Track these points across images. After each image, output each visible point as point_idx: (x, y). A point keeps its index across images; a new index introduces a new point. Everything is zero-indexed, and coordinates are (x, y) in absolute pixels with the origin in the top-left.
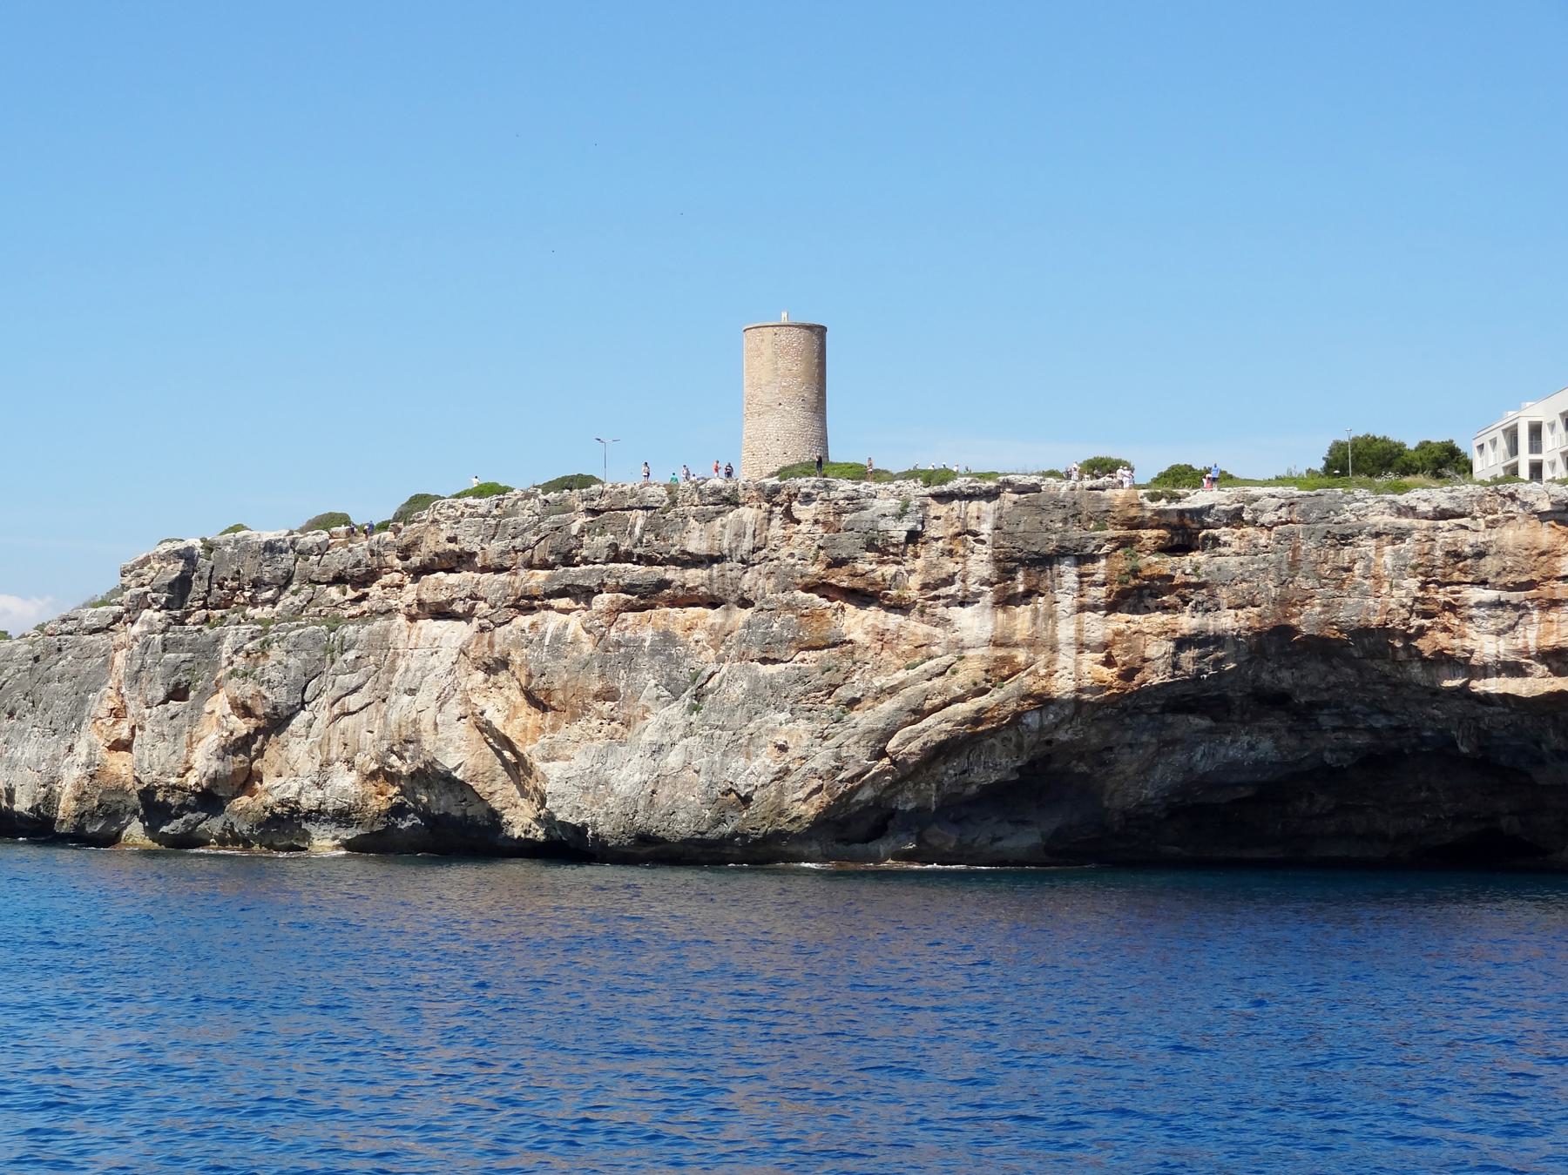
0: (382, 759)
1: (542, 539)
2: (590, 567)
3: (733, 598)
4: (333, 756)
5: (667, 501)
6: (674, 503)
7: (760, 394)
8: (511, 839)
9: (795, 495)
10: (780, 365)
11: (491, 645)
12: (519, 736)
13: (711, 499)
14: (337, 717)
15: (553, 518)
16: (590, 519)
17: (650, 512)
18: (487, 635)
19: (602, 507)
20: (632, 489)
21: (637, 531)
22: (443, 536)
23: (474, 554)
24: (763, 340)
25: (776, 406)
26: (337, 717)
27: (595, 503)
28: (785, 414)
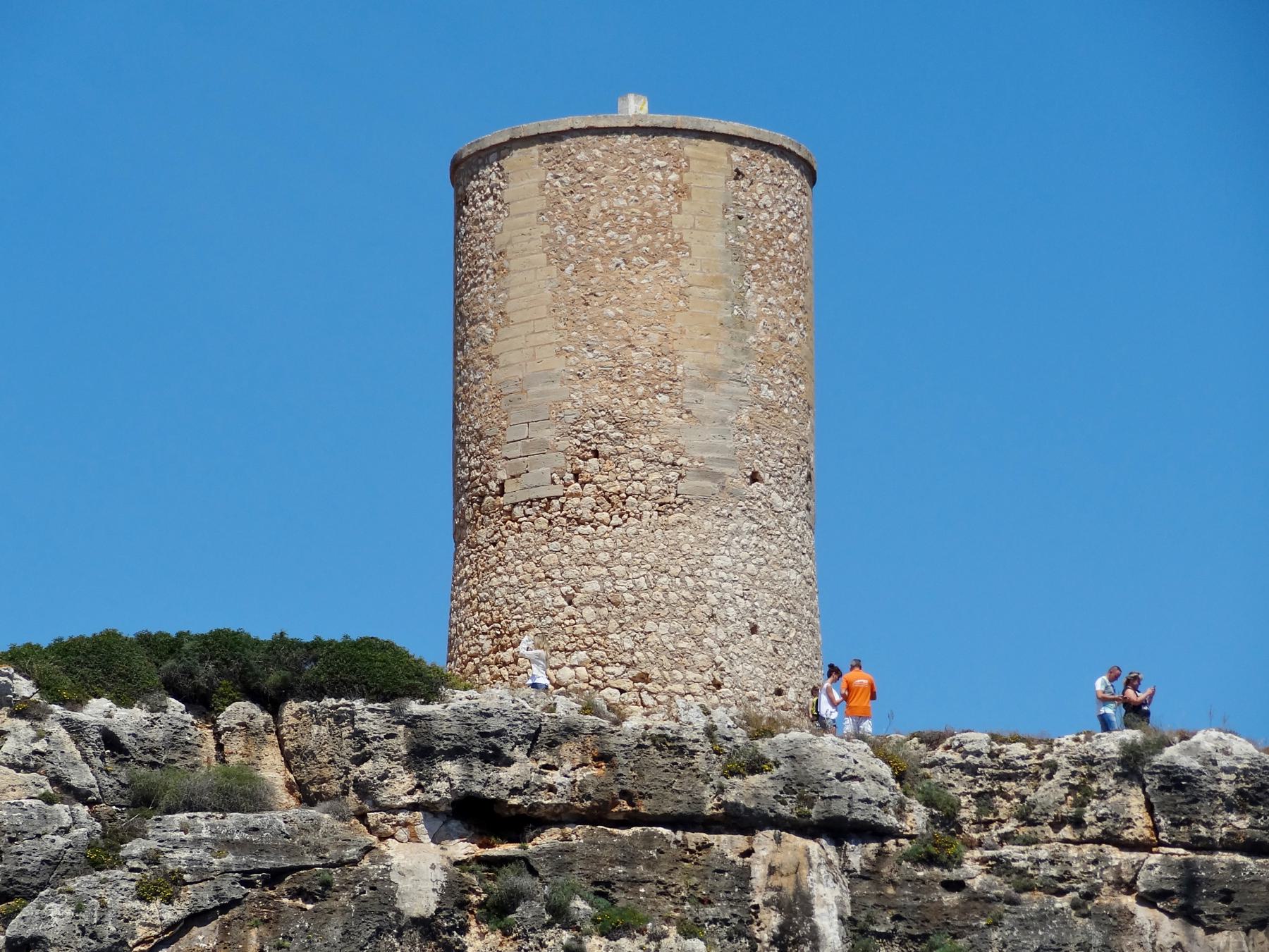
1: (198, 918)
5: (917, 818)
6: (946, 819)
7: (669, 417)
10: (753, 310)
13: (1243, 823)
15: (203, 823)
16: (462, 849)
17: (858, 855)
19: (545, 799)
20: (710, 732)
21: (828, 923)
24: (682, 191)
25: (741, 484)
27: (508, 775)
28: (771, 522)
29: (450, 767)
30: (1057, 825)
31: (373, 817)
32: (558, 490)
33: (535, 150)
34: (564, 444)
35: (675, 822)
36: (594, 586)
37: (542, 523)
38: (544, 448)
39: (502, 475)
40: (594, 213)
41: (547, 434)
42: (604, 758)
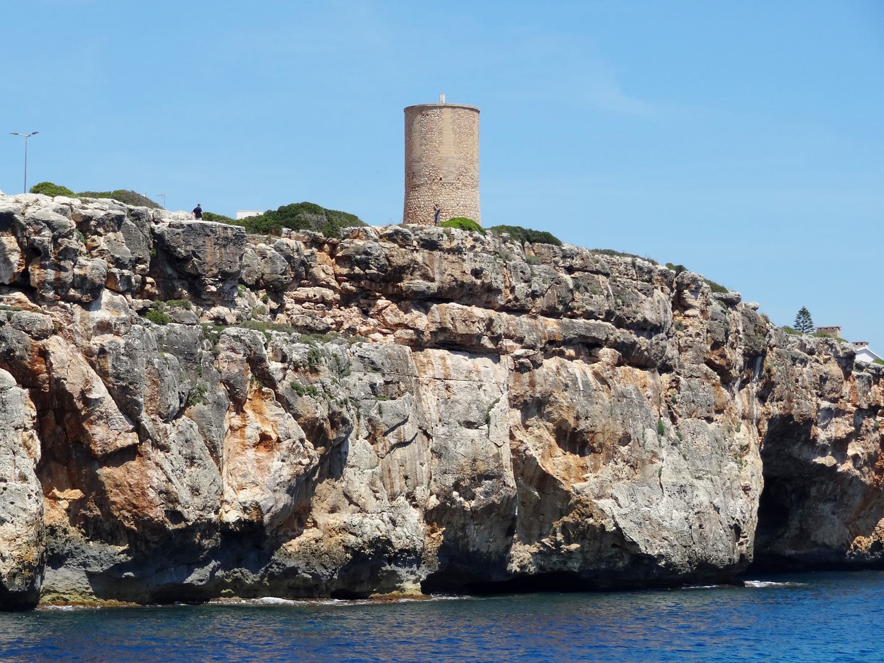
0: (445, 496)
2: (592, 321)
3: (659, 363)
4: (397, 489)
8: (509, 573)
9: (688, 286)
11: (532, 384)
12: (563, 474)
14: (393, 447)
18: (526, 375)
22: (468, 267)
23: (499, 291)
26: (393, 447)
29: (569, 260)
30: (624, 275)
31: (557, 268)
32: (455, 182)
33: (450, 109)
34: (456, 172)
35: (592, 272)
36: (462, 203)
37: (451, 188)
38: (452, 172)
39: (441, 176)
40: (462, 125)
41: (453, 170)
42: (582, 259)
